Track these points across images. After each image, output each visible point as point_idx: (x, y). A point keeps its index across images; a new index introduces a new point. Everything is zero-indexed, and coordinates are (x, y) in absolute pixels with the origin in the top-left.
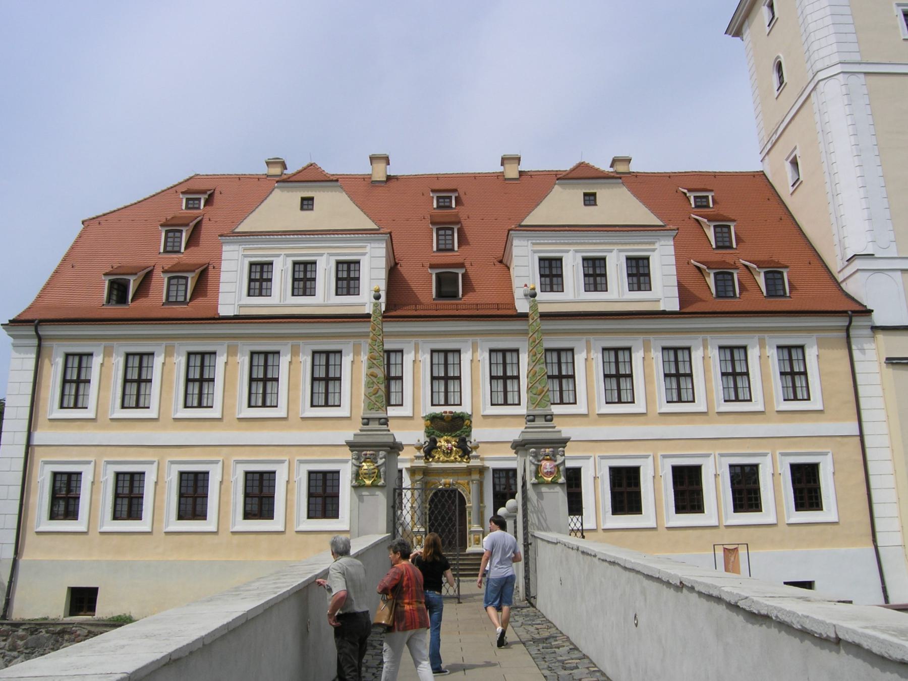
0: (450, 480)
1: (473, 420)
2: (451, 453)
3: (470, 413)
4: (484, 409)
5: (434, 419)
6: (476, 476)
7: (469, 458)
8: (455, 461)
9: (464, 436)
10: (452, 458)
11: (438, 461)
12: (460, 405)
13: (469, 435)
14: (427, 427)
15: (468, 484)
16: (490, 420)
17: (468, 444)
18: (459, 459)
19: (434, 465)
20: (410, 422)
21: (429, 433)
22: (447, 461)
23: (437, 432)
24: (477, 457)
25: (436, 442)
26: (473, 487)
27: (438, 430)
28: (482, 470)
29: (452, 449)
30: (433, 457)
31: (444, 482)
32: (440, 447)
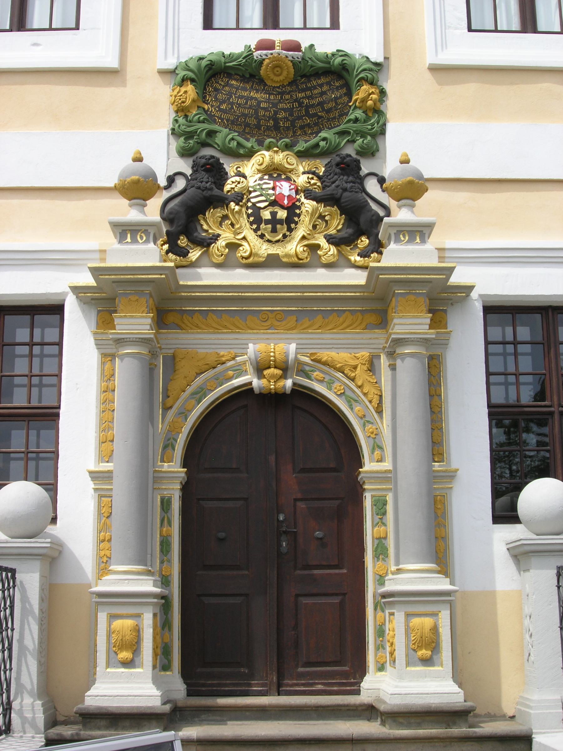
0: (288, 347)
1: (390, 85)
2: (291, 222)
3: (377, 56)
4: (442, 43)
5: (211, 75)
6: (410, 323)
7: (378, 247)
8: (311, 258)
9: (350, 151)
10: (293, 247)
11: (231, 258)
12: (335, 25)
13: (370, 152)
14: (182, 110)
15: (372, 367)
16: (470, 89)
17: (372, 187)
18: (329, 251)
19: (210, 276)
20: (106, 93)
21: (190, 138)
22: (272, 262)
23: (224, 135)
24: (418, 232)
25: (217, 173)
26: (403, 381)
27: (232, 124)
28: (439, 296)
29: (293, 209)
30: (206, 243)
31: (250, 358)
32: (239, 198)
